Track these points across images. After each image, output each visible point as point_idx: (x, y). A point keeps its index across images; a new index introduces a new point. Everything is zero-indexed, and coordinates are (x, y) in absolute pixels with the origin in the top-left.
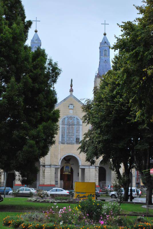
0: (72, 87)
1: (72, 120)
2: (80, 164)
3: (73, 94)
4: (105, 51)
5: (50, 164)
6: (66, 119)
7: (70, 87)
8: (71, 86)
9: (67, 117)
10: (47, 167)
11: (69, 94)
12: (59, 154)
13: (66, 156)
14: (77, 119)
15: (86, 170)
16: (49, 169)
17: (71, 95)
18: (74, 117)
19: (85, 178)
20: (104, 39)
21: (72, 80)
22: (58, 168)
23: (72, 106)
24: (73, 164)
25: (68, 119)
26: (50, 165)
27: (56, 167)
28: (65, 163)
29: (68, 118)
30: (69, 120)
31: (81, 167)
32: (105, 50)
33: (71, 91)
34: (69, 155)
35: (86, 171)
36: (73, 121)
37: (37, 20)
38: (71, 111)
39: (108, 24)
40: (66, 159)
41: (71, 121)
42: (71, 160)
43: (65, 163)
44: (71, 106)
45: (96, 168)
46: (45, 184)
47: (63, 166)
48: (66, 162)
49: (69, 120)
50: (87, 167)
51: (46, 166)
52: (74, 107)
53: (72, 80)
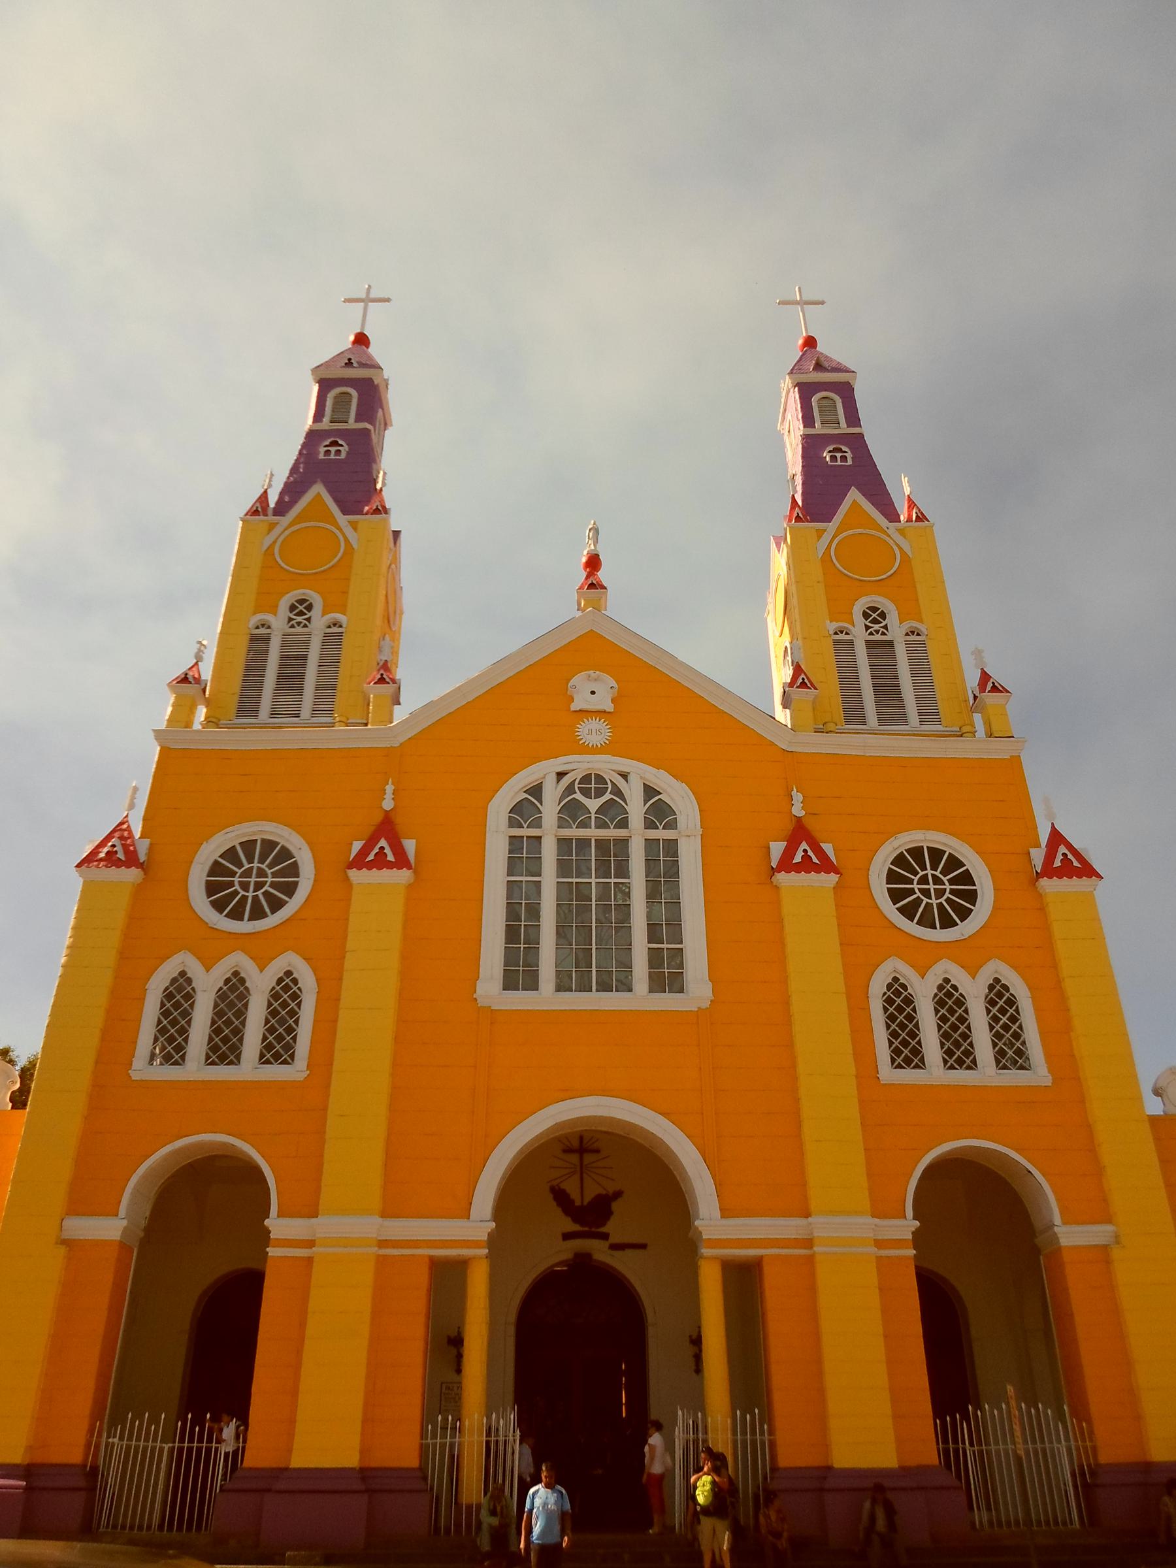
0: (602, 575)
1: (608, 796)
4: (825, 403)
8: (593, 563)
9: (560, 775)
14: (650, 791)
15: (767, 1269)
18: (625, 776)
24: (643, 1246)
25: (570, 789)
28: (567, 1236)
29: (566, 781)
30: (578, 796)
37: (372, 296)
39: (822, 303)
40: (575, 1195)
41: (593, 805)
42: (615, 1206)
43: (567, 1236)
46: (298, 1461)
48: (577, 1228)
49: (578, 796)
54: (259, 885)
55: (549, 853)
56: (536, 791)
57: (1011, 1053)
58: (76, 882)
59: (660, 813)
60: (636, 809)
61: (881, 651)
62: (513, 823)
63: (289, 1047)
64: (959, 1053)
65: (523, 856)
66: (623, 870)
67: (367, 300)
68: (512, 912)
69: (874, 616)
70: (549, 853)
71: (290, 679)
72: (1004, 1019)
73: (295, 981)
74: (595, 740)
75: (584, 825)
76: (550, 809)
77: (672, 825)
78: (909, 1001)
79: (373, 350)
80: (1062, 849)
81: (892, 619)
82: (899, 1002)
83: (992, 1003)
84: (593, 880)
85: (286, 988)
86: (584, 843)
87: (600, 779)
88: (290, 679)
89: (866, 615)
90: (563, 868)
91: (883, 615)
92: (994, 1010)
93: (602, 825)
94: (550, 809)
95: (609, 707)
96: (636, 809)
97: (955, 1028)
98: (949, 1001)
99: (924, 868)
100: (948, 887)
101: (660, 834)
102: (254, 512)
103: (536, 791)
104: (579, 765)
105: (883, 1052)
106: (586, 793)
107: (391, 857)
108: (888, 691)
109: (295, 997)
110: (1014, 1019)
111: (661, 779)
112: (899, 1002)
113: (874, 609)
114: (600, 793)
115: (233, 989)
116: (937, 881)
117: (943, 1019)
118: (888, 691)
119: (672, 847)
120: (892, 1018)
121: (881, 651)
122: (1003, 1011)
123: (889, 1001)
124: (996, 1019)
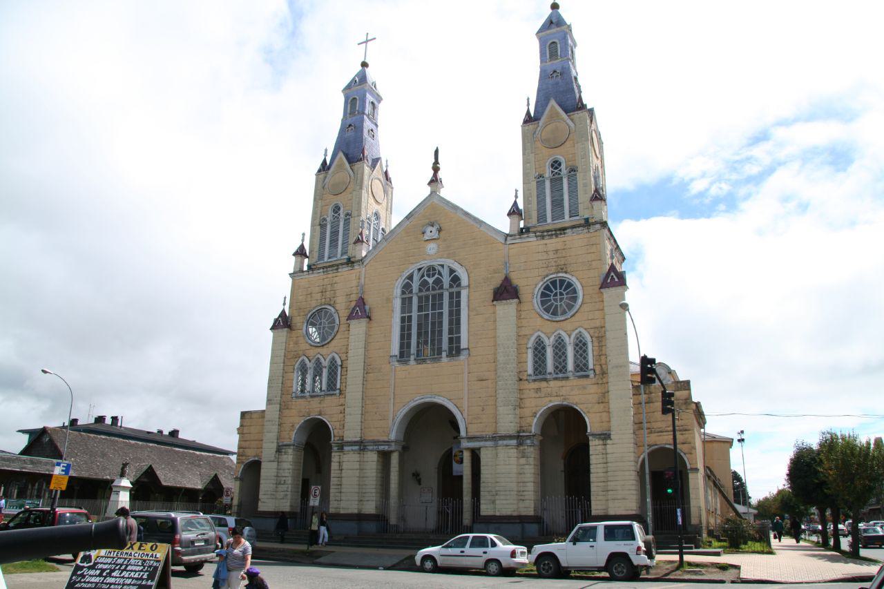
0: (440, 174)
1: (436, 276)
2: (463, 433)
3: (444, 193)
5: (358, 439)
6: (416, 278)
7: (432, 172)
8: (436, 169)
9: (420, 269)
10: (350, 448)
11: (427, 191)
12: (392, 400)
13: (413, 404)
14: (452, 271)
16: (356, 457)
17: (433, 193)
18: (442, 266)
19: (482, 485)
20: (550, 16)
21: (437, 152)
22: (391, 452)
23: (434, 229)
25: (423, 276)
26: (362, 445)
27: (381, 448)
30: (426, 278)
31: (465, 444)
32: (554, 42)
33: (435, 181)
34: (423, 400)
35: (485, 457)
36: (438, 278)
38: (432, 248)
41: (431, 280)
44: (430, 228)
45: (520, 444)
47: (449, 447)
49: (426, 278)
50: (489, 443)
51: (346, 448)
52: (440, 230)
53: (437, 152)
54: (324, 328)
55: (415, 300)
56: (410, 277)
57: (581, 367)
58: (270, 335)
59: (455, 280)
60: (446, 280)
61: (556, 181)
62: (403, 293)
63: (335, 385)
64: (561, 367)
65: (406, 303)
66: (441, 307)
67: (366, 42)
68: (402, 329)
69: (556, 164)
70: (415, 300)
71: (334, 242)
72: (581, 352)
73: (336, 362)
74: (432, 252)
75: (428, 290)
76: (415, 286)
77: (459, 285)
78: (544, 348)
79: (368, 70)
80: (612, 274)
81: (563, 166)
82: (539, 349)
83: (577, 345)
84: (430, 312)
85: (333, 365)
86: (427, 297)
87: (434, 269)
88: (334, 242)
89: (552, 166)
90: (420, 309)
91: (560, 164)
92: (577, 348)
93: (434, 289)
94: (415, 286)
95: (436, 236)
96: (446, 280)
97: (560, 357)
98: (560, 347)
99: (556, 289)
100: (565, 296)
101: (455, 290)
102: (319, 171)
103: (410, 277)
104: (425, 264)
105: (530, 370)
106: (429, 277)
107: (360, 314)
108: (557, 204)
109: (336, 367)
110: (585, 351)
111: (456, 266)
112: (539, 349)
113: (556, 162)
114: (433, 275)
115: (318, 366)
116: (561, 294)
117: (556, 354)
118: (557, 204)
119: (459, 294)
120: (535, 356)
121: (556, 181)
122: (581, 348)
123: (536, 349)
124: (577, 352)
